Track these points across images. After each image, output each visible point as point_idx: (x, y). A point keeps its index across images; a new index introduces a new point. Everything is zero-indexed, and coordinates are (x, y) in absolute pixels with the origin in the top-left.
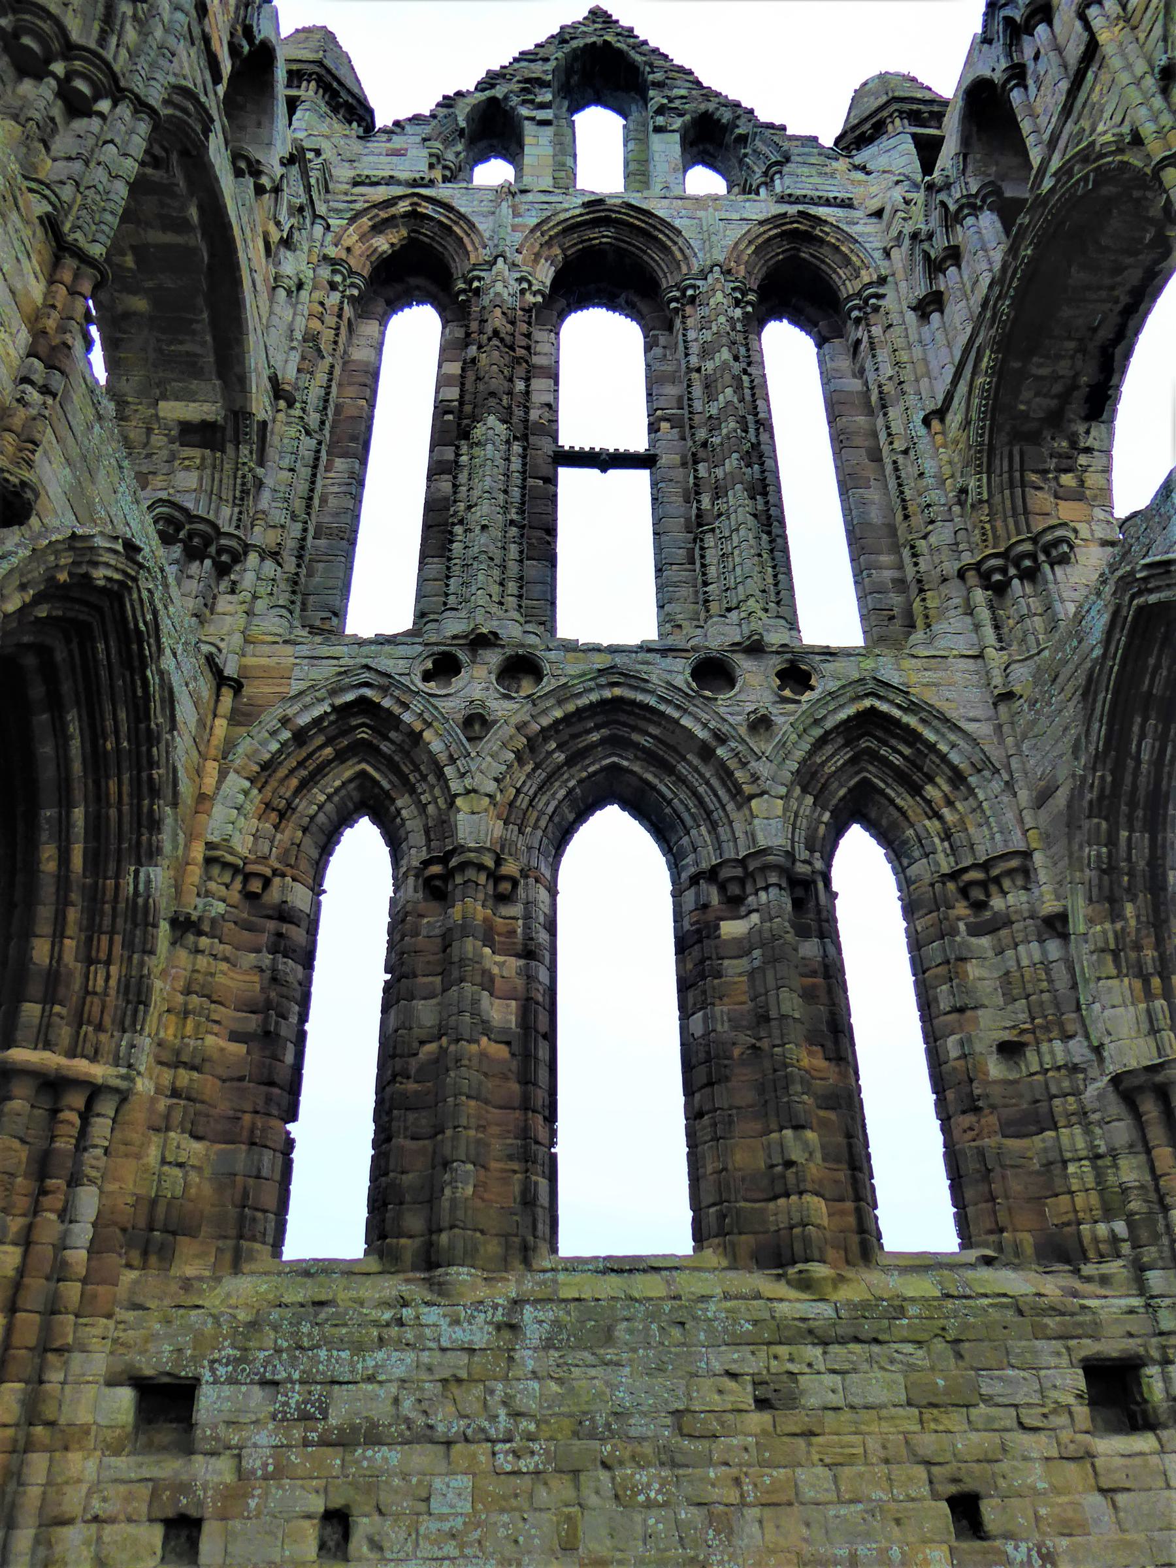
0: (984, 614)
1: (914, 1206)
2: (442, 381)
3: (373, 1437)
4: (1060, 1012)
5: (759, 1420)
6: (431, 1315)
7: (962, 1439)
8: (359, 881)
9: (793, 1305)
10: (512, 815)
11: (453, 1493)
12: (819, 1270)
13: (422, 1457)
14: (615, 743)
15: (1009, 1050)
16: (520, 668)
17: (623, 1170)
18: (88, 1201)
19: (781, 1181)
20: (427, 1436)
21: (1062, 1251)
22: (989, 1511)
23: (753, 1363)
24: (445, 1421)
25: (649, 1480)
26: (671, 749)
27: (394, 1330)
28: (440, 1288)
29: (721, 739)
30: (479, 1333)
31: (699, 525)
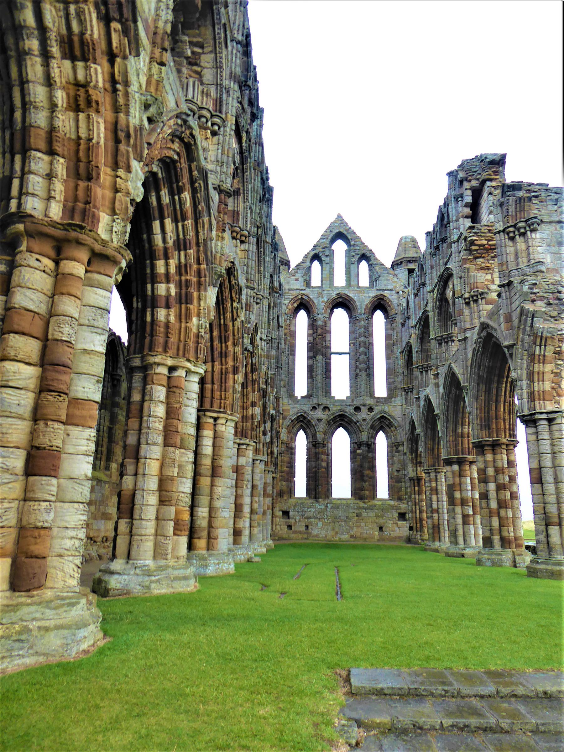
0: (404, 397)
1: (383, 490)
2: (309, 335)
3: (310, 518)
4: (404, 468)
5: (356, 518)
6: (317, 505)
7: (381, 521)
9: (362, 505)
10: (325, 433)
12: (366, 501)
13: (316, 520)
15: (398, 471)
16: (326, 408)
17: (341, 485)
19: (362, 489)
21: (400, 499)
23: (356, 511)
24: (319, 516)
25: (343, 524)
26: (350, 422)
27: (312, 507)
28: (318, 502)
29: (358, 422)
30: (323, 507)
31: (357, 375)
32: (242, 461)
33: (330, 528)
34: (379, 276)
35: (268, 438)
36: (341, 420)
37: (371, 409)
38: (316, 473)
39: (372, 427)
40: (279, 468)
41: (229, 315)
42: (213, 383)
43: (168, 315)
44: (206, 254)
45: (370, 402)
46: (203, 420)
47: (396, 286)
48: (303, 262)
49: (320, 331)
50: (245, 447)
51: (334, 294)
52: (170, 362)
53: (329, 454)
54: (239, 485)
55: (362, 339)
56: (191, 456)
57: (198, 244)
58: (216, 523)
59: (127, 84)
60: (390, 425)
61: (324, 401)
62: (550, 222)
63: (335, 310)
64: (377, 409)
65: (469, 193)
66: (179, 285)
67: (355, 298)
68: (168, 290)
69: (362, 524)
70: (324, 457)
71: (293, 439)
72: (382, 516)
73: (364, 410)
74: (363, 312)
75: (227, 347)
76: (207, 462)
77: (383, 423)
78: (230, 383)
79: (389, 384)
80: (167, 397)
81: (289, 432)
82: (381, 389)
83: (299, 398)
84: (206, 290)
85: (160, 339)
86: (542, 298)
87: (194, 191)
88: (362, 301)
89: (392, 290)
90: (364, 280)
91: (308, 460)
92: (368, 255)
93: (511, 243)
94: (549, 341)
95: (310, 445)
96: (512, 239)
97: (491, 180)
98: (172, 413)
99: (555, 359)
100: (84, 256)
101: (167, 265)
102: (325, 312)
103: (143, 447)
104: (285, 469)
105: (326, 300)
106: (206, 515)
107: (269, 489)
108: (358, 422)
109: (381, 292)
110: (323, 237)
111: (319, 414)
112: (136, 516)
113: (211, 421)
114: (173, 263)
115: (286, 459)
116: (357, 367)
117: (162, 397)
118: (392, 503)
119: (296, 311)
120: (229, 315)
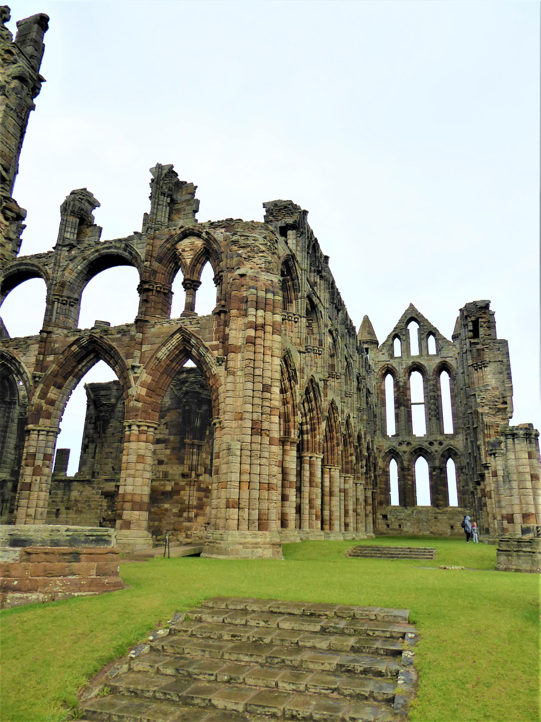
1: (453, 500)
2: (395, 392)
3: (402, 520)
4: (467, 485)
7: (452, 522)
8: (393, 467)
10: (409, 461)
11: (409, 524)
13: (406, 521)
14: (420, 451)
16: (409, 444)
17: (423, 497)
18: (376, 501)
19: (438, 500)
20: (406, 520)
21: (465, 507)
22: (454, 527)
23: (434, 515)
24: (408, 519)
25: (425, 524)
28: (407, 509)
29: (432, 452)
30: (410, 512)
31: (430, 419)
32: (347, 486)
33: (415, 527)
34: (442, 348)
35: (364, 470)
36: (420, 452)
37: (441, 444)
38: (404, 488)
39: (443, 456)
40: (378, 486)
41: (333, 420)
42: (328, 452)
43: (308, 437)
44: (320, 410)
45: (440, 438)
46: (324, 470)
47: (452, 356)
48: (386, 341)
49: (401, 389)
50: (348, 478)
51: (410, 363)
52: (310, 455)
53: (413, 476)
54: (346, 499)
55: (432, 394)
56: (320, 490)
57: (317, 408)
58: (333, 518)
59: (295, 393)
60: (456, 454)
61: (407, 439)
62: (495, 362)
63: (413, 373)
64: (445, 443)
65: (471, 324)
66: (311, 424)
67: (426, 365)
68: (307, 427)
69: (439, 524)
70: (409, 478)
71: (388, 465)
72: (453, 519)
73: (436, 444)
74: (431, 374)
75: (333, 435)
76: (327, 489)
77: (450, 453)
78: (336, 451)
79: (454, 424)
80: (310, 468)
81: (384, 461)
82: (448, 428)
83: (390, 436)
84: (321, 424)
85: (306, 446)
86: (487, 405)
87: (314, 391)
88: (431, 366)
89: (452, 357)
90: (432, 350)
91: (399, 480)
92: (434, 332)
93: (476, 372)
94: (491, 427)
95: (399, 469)
96: (476, 370)
97: (482, 318)
98: (312, 474)
99: (496, 435)
100: (289, 444)
101: (306, 418)
102: (405, 376)
103: (302, 487)
104: (383, 486)
105: (404, 367)
106: (328, 514)
107: (370, 501)
108: (432, 452)
109: (444, 359)
110: (401, 321)
111: (404, 448)
112: (302, 513)
113: (328, 470)
114: (308, 417)
115: (383, 479)
116: (430, 414)
117: (308, 468)
118: (460, 509)
119: (384, 375)
120: (333, 420)
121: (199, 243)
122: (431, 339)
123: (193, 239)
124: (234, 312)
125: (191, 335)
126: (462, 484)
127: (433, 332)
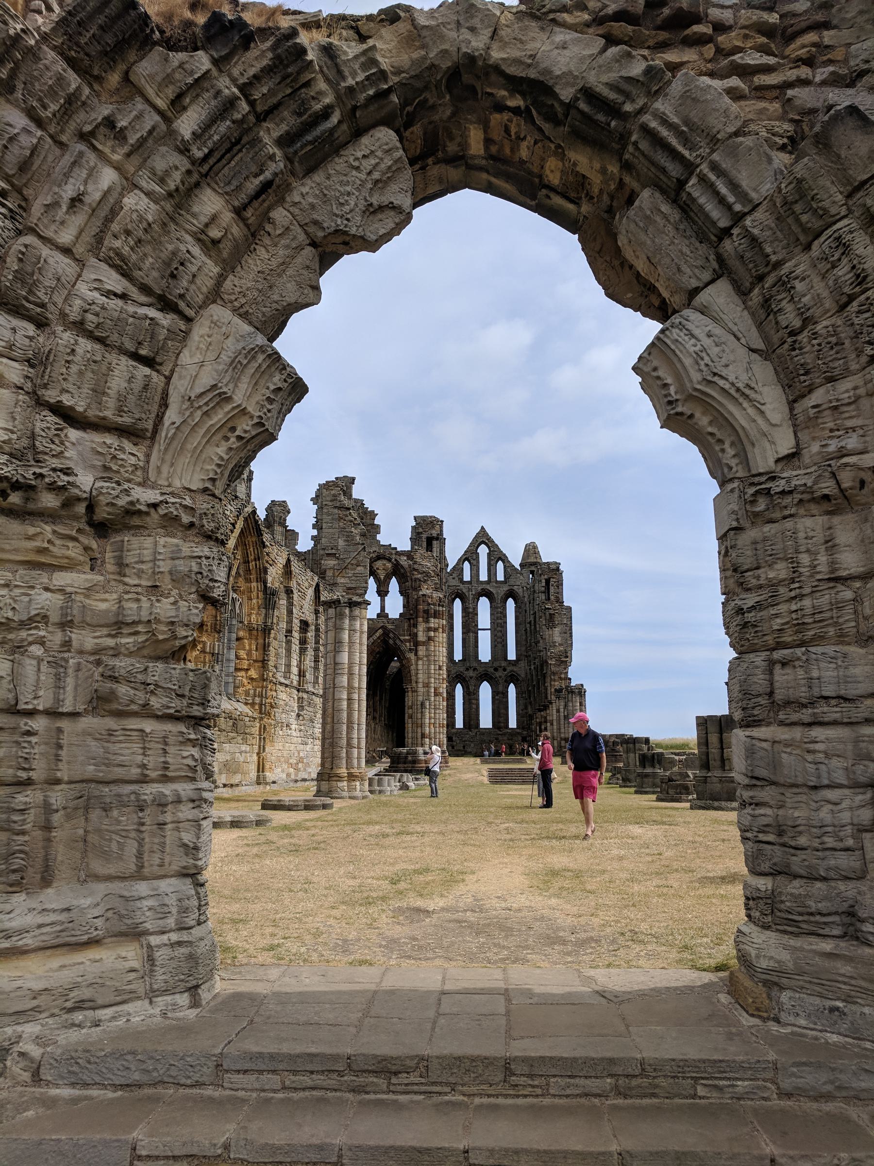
16: (475, 669)
17: (486, 720)
36: (485, 676)
45: (504, 664)
53: (478, 700)
60: (518, 680)
61: (475, 664)
64: (509, 669)
73: (500, 670)
82: (512, 655)
90: (500, 577)
111: (471, 673)
119: (454, 600)
121: (389, 565)
122: (500, 565)
123: (385, 562)
124: (420, 619)
125: (390, 631)
126: (522, 707)
127: (503, 558)
